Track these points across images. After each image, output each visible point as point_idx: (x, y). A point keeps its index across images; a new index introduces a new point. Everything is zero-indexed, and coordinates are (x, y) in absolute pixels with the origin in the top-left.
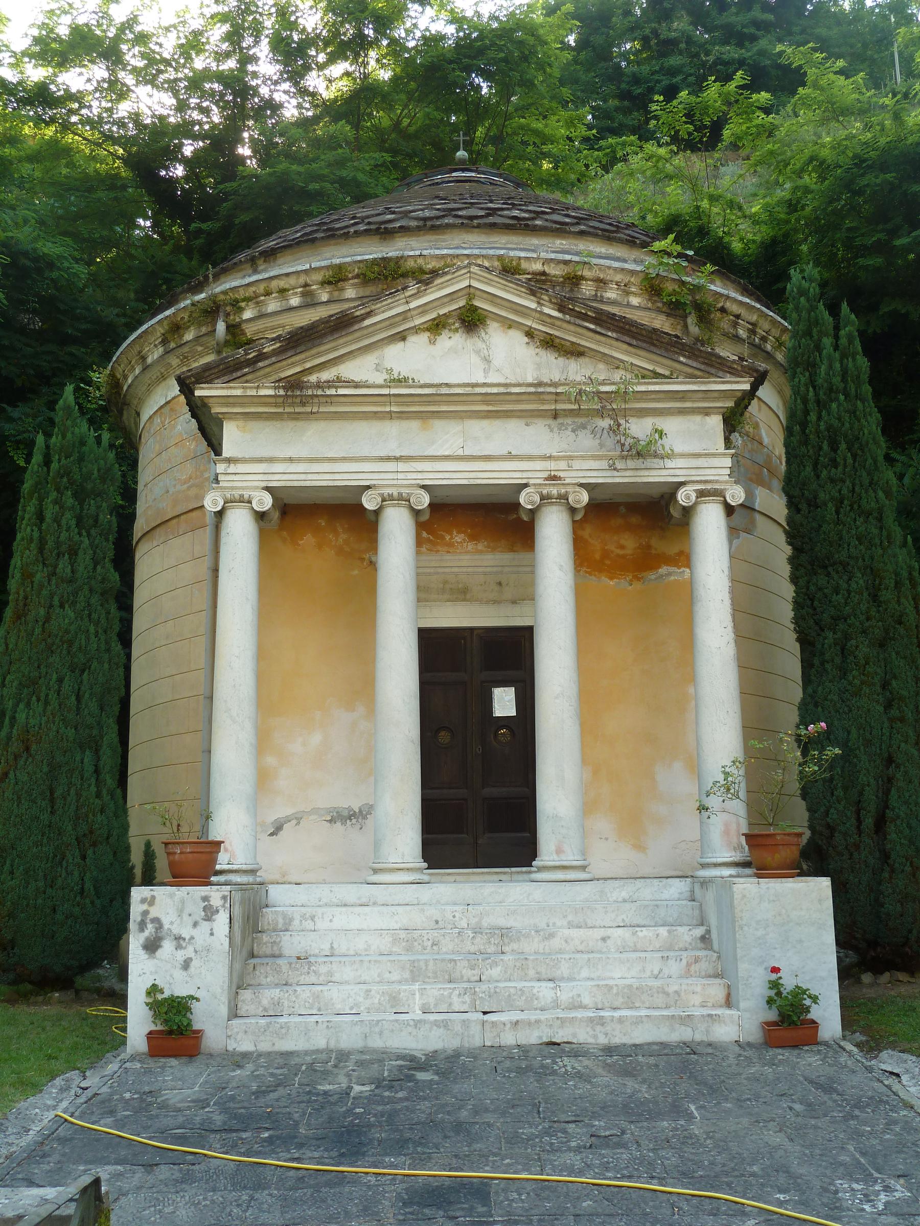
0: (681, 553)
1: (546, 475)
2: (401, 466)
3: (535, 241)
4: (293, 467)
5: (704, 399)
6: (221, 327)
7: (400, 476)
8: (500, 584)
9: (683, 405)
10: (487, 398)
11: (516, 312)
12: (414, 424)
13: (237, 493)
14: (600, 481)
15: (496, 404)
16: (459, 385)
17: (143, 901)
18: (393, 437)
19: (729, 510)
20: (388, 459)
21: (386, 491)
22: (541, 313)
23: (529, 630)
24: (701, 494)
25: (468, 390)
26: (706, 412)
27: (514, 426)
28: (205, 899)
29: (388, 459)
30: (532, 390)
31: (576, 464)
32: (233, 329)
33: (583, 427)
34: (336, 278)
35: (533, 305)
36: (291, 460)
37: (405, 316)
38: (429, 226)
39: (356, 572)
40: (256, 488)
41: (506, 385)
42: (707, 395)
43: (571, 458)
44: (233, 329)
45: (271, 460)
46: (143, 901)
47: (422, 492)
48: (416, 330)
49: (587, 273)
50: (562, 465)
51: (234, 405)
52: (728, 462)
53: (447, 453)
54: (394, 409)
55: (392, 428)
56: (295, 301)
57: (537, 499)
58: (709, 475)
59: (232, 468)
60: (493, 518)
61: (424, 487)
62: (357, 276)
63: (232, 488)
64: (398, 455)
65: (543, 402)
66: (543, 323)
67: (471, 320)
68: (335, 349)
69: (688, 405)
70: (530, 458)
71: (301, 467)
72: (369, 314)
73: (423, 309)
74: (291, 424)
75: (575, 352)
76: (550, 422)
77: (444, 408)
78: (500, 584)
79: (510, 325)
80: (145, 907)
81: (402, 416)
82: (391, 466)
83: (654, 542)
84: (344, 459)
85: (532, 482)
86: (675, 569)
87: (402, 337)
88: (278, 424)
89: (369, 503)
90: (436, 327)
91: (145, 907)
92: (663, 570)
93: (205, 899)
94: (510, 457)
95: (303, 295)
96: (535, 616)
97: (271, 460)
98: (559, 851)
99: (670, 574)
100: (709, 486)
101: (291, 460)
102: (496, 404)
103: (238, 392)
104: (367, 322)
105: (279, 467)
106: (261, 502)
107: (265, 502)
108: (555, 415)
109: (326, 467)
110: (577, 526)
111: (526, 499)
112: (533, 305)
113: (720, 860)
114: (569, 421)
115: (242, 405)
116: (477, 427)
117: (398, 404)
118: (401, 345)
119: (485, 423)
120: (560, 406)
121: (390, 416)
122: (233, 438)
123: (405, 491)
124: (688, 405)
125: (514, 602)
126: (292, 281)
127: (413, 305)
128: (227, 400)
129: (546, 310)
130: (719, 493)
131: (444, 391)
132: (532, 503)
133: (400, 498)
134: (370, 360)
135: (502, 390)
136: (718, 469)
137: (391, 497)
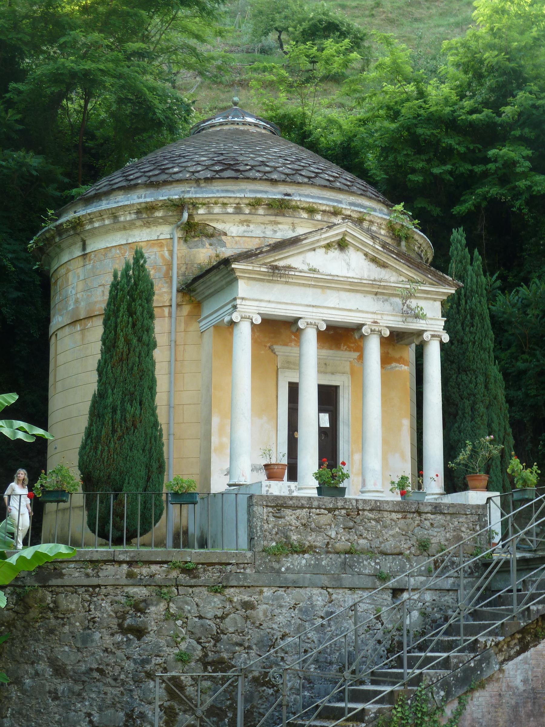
0: (401, 357)
1: (372, 320)
2: (315, 310)
4: (270, 305)
5: (436, 295)
6: (186, 215)
7: (314, 314)
8: (326, 364)
9: (428, 296)
11: (363, 245)
12: (319, 291)
13: (247, 315)
14: (393, 326)
15: (354, 286)
16: (342, 277)
17: (267, 486)
18: (309, 296)
20: (310, 306)
21: (309, 321)
22: (374, 247)
23: (336, 388)
24: (433, 336)
25: (345, 279)
26: (435, 300)
27: (359, 296)
28: (289, 487)
29: (310, 306)
30: (371, 282)
31: (385, 317)
33: (387, 300)
35: (372, 244)
36: (269, 301)
37: (318, 241)
39: (263, 352)
40: (255, 313)
41: (361, 279)
42: (437, 293)
43: (383, 314)
45: (261, 301)
46: (267, 486)
47: (323, 322)
48: (320, 247)
49: (367, 218)
50: (379, 317)
51: (245, 273)
52: (443, 323)
53: (332, 306)
54: (313, 283)
55: (310, 291)
57: (369, 331)
58: (436, 328)
59: (244, 302)
60: (340, 336)
61: (324, 320)
62: (267, 205)
63: (244, 312)
64: (314, 304)
65: (373, 288)
66: (374, 251)
67: (342, 245)
68: (288, 252)
69: (429, 296)
70: (367, 312)
71: (273, 305)
72: (305, 239)
73: (325, 239)
74: (267, 284)
75: (384, 266)
76: (374, 296)
77: (333, 285)
78: (326, 364)
79: (358, 249)
80: (267, 488)
81: (314, 286)
82: (310, 309)
83: (390, 351)
84: (292, 304)
85: (368, 323)
86: (397, 365)
87: (314, 250)
88: (262, 283)
90: (328, 246)
91: (267, 488)
92: (394, 365)
93: (289, 487)
94: (357, 311)
95: (235, 208)
97: (261, 301)
98: (375, 484)
99: (396, 367)
100: (436, 333)
101: (269, 301)
102: (354, 286)
103: (251, 268)
104: (304, 242)
105: (263, 304)
106: (256, 320)
108: (376, 294)
109: (283, 306)
110: (382, 344)
112: (372, 244)
113: (435, 492)
114: (381, 297)
115: (249, 273)
116: (345, 295)
117: (315, 281)
118: (313, 253)
119: (348, 294)
120: (379, 290)
121: (309, 286)
122: (243, 288)
123: (316, 321)
124: (429, 296)
125: (333, 374)
126: (231, 200)
127: (324, 236)
128: (243, 271)
129: (377, 247)
131: (336, 278)
132: (367, 333)
133: (315, 325)
134: (300, 258)
135: (359, 281)
137: (311, 324)
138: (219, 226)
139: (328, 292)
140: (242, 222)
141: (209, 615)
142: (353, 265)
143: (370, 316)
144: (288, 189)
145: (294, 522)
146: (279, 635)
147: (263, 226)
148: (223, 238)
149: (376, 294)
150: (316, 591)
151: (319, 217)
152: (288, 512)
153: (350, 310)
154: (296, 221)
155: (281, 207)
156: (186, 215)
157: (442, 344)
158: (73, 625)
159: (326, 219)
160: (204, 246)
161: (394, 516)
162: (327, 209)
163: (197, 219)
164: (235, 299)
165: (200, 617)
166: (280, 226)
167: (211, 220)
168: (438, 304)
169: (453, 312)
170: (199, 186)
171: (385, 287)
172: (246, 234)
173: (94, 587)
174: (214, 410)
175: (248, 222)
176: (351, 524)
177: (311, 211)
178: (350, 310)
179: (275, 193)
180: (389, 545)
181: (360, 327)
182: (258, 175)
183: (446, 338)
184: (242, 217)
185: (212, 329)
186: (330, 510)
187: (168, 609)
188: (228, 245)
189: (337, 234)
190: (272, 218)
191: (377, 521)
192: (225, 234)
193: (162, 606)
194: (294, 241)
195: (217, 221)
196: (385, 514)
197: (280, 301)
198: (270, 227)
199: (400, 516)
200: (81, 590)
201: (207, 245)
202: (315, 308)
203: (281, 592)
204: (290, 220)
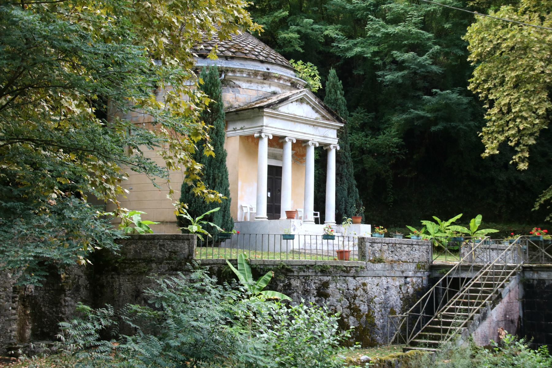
10: (306, 120)
12: (293, 123)
18: (289, 126)
24: (334, 147)
26: (334, 129)
27: (308, 126)
50: (314, 137)
52: (337, 141)
55: (290, 123)
56: (245, 75)
67: (301, 101)
75: (317, 111)
79: (308, 103)
81: (291, 121)
87: (292, 102)
90: (297, 101)
96: (283, 164)
108: (314, 125)
116: (302, 125)
126: (246, 71)
128: (267, 112)
134: (286, 106)
138: (237, 83)
139: (296, 123)
140: (248, 81)
141: (352, 289)
142: (305, 111)
143: (311, 136)
145: (377, 249)
146: (373, 296)
147: (257, 84)
148: (239, 88)
150: (383, 278)
151: (281, 82)
152: (376, 245)
153: (305, 133)
154: (272, 83)
155: (266, 76)
156: (223, 76)
157: (336, 150)
158: (298, 293)
159: (284, 83)
160: (229, 92)
161: (406, 246)
162: (286, 78)
164: (262, 126)
165: (348, 289)
166: (265, 85)
167: (234, 79)
168: (335, 132)
169: (341, 134)
170: (227, 59)
171: (318, 122)
172: (250, 88)
173: (306, 276)
174: (239, 179)
175: (251, 82)
176: (393, 250)
177: (279, 78)
178: (305, 133)
179: (263, 68)
180: (404, 258)
181: (308, 141)
183: (338, 148)
184: (249, 79)
185: (238, 137)
186: (387, 244)
187: (336, 286)
188: (241, 93)
190: (262, 81)
191: (400, 248)
192: (240, 87)
193: (334, 284)
194: (286, 99)
195: (236, 80)
196: (403, 245)
198: (260, 85)
199: (406, 246)
200: (301, 278)
201: (231, 92)
202: (293, 132)
203: (374, 279)
204: (269, 82)
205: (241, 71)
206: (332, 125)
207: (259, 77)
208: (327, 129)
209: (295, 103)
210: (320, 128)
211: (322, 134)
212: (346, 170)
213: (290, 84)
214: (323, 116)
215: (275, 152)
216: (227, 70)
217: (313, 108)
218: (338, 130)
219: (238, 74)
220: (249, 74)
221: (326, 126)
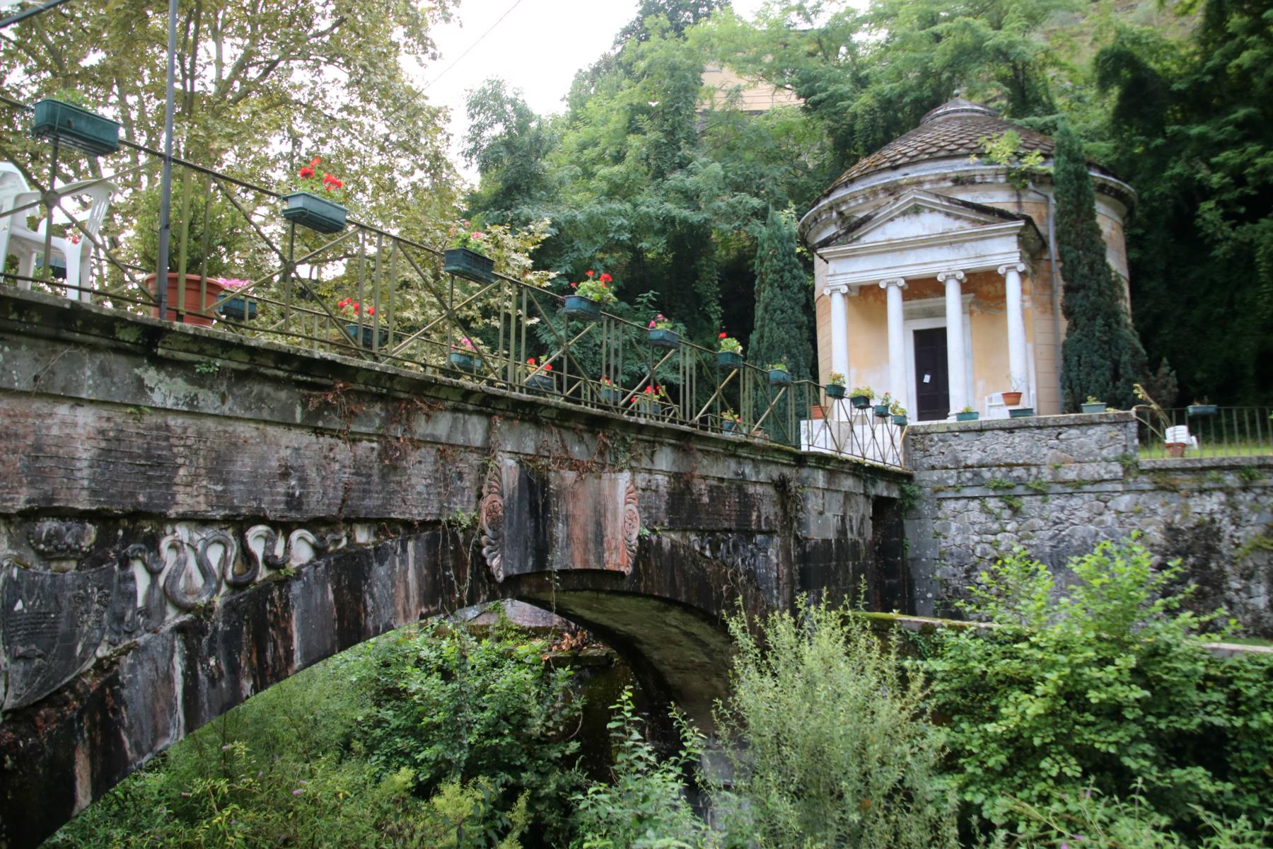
3: (956, 162)
6: (834, 214)
10: (922, 241)
12: (898, 253)
18: (889, 260)
19: (1020, 274)
26: (1010, 235)
27: (935, 249)
32: (840, 214)
34: (874, 192)
37: (891, 212)
38: (913, 162)
44: (840, 214)
55: (889, 256)
67: (917, 210)
73: (898, 209)
75: (958, 217)
79: (932, 210)
87: (892, 220)
89: (882, 286)
90: (904, 214)
107: (845, 289)
108: (951, 243)
111: (940, 279)
116: (920, 252)
118: (890, 225)
121: (888, 252)
130: (1015, 267)
134: (879, 231)
136: (1015, 258)
144: (906, 170)
149: (951, 243)
151: (927, 186)
163: (846, 213)
168: (1014, 238)
171: (955, 236)
177: (919, 183)
179: (897, 176)
182: (888, 164)
189: (908, 202)
197: (862, 270)
202: (889, 271)
205: (854, 197)
206: (999, 230)
207: (881, 196)
208: (988, 242)
209: (899, 221)
210: (967, 245)
211: (972, 254)
212: (1085, 303)
213: (950, 184)
214: (974, 221)
215: (926, 306)
216: (838, 205)
217: (948, 214)
218: (1019, 235)
219: (853, 204)
220: (866, 198)
221: (983, 237)
